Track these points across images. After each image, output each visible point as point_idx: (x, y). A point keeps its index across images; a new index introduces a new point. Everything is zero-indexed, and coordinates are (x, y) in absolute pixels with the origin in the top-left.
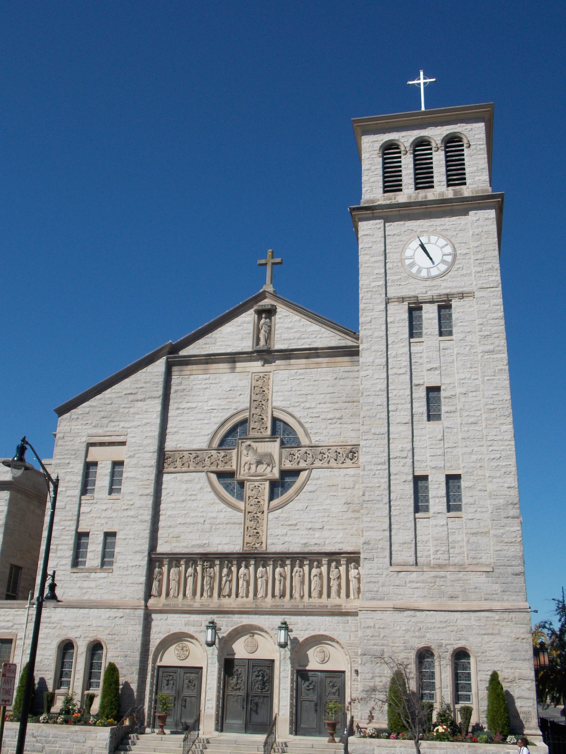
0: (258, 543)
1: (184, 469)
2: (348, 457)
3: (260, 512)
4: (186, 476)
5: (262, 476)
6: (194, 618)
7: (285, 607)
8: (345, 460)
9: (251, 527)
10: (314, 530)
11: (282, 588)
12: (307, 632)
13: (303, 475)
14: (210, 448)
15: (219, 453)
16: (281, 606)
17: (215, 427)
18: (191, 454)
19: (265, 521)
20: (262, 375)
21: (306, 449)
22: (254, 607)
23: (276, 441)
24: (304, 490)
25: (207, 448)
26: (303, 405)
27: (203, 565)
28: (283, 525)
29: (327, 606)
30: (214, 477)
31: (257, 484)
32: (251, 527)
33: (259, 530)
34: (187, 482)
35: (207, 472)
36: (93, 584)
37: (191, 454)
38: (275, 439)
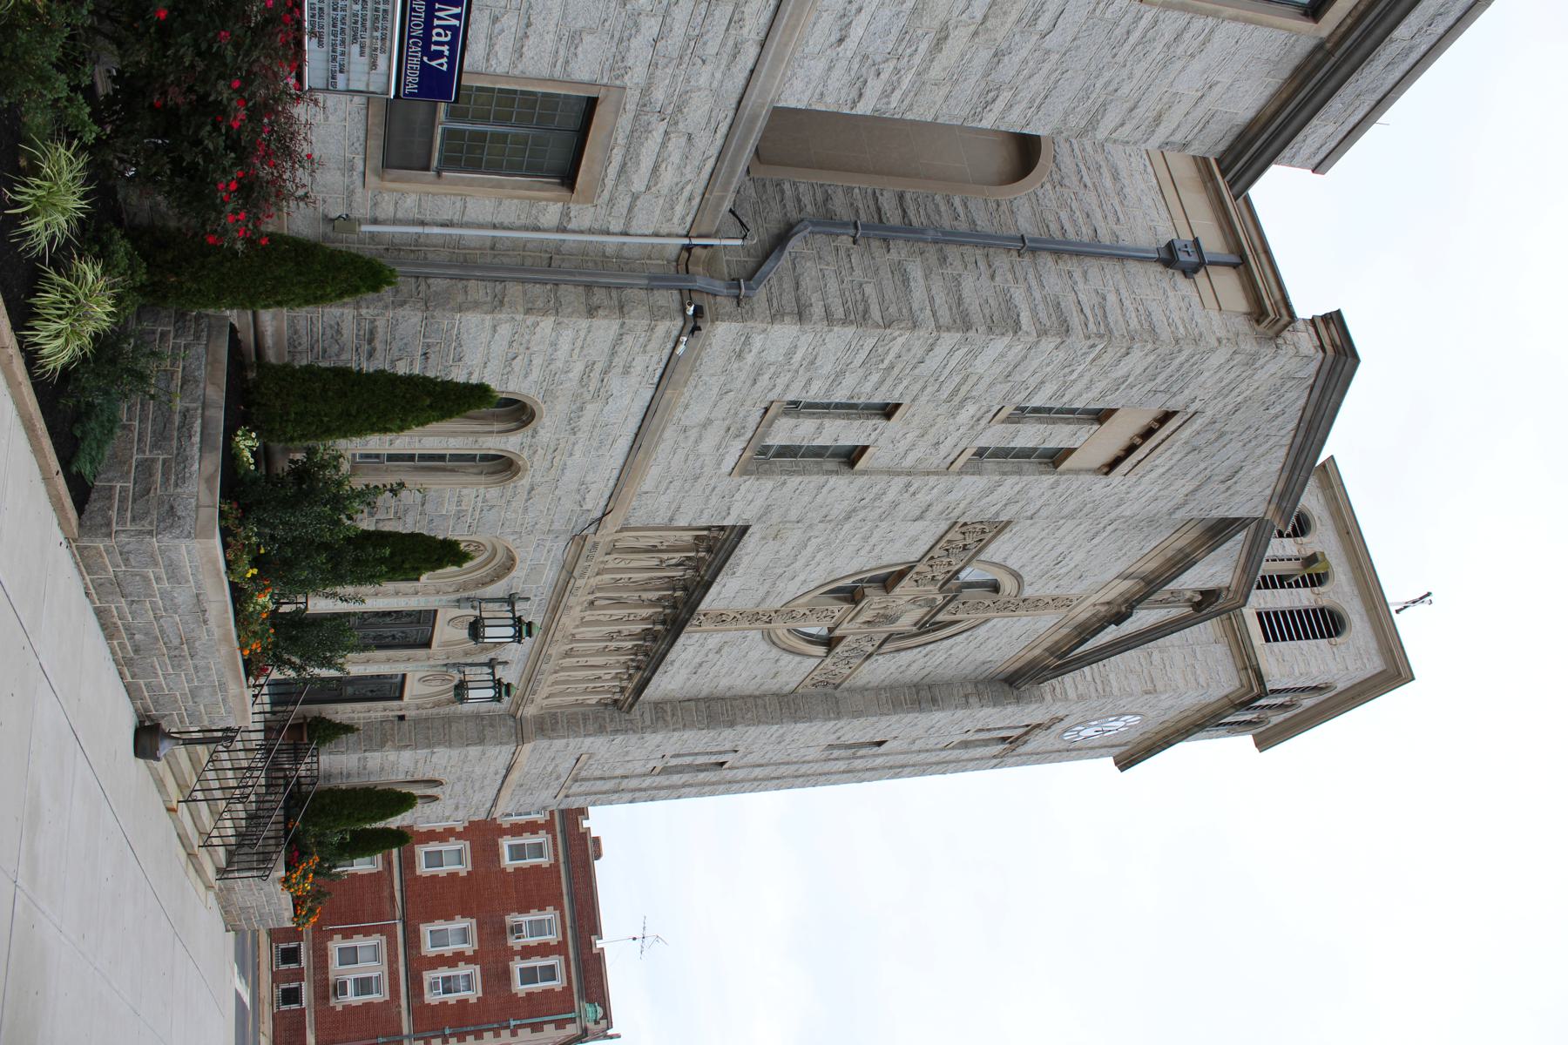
36: (707, 446)
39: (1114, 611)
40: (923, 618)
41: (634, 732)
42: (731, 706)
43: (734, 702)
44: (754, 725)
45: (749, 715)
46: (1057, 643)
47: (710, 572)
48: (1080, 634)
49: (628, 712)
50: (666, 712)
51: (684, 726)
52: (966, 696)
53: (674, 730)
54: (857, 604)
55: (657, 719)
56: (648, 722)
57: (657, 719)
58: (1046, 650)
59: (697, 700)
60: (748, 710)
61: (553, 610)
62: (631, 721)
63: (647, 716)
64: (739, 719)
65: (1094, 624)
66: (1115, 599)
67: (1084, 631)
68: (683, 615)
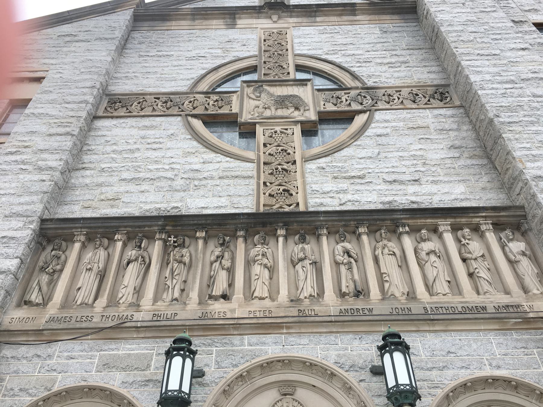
0: (290, 206)
1: (142, 113)
2: (434, 98)
3: (288, 163)
4: (147, 122)
5: (287, 118)
6: (129, 349)
7: (374, 312)
8: (429, 101)
9: (271, 183)
10: (402, 182)
11: (356, 277)
12: (449, 373)
13: (360, 120)
14: (192, 91)
15: (209, 98)
16: (366, 312)
17: (203, 72)
18: (158, 99)
19: (298, 174)
20: (275, 31)
21: (358, 91)
22: (296, 314)
23: (306, 85)
24: (366, 134)
25: (188, 91)
26: (343, 52)
27: (165, 241)
28: (335, 178)
29: (484, 308)
30: (198, 124)
31: (278, 129)
32: (271, 183)
33: (289, 187)
34: (146, 127)
35: (186, 115)
37: (158, 99)
38: (305, 83)
39: (272, 11)
40: (292, 85)
41: (530, 188)
42: (485, 135)
43: (482, 136)
44: (485, 107)
45: (483, 117)
46: (340, 15)
47: (153, 223)
48: (316, 11)
49: (522, 207)
50: (509, 179)
51: (508, 154)
52: (426, 18)
53: (514, 158)
54: (254, 124)
55: (515, 179)
56: (521, 184)
57: (515, 179)
58: (355, 15)
59: (492, 162)
60: (482, 121)
61: (224, 329)
62: (526, 199)
63: (517, 190)
64: (487, 120)
65: (298, 12)
66: (266, 18)
67: (313, 11)
68: (244, 221)
